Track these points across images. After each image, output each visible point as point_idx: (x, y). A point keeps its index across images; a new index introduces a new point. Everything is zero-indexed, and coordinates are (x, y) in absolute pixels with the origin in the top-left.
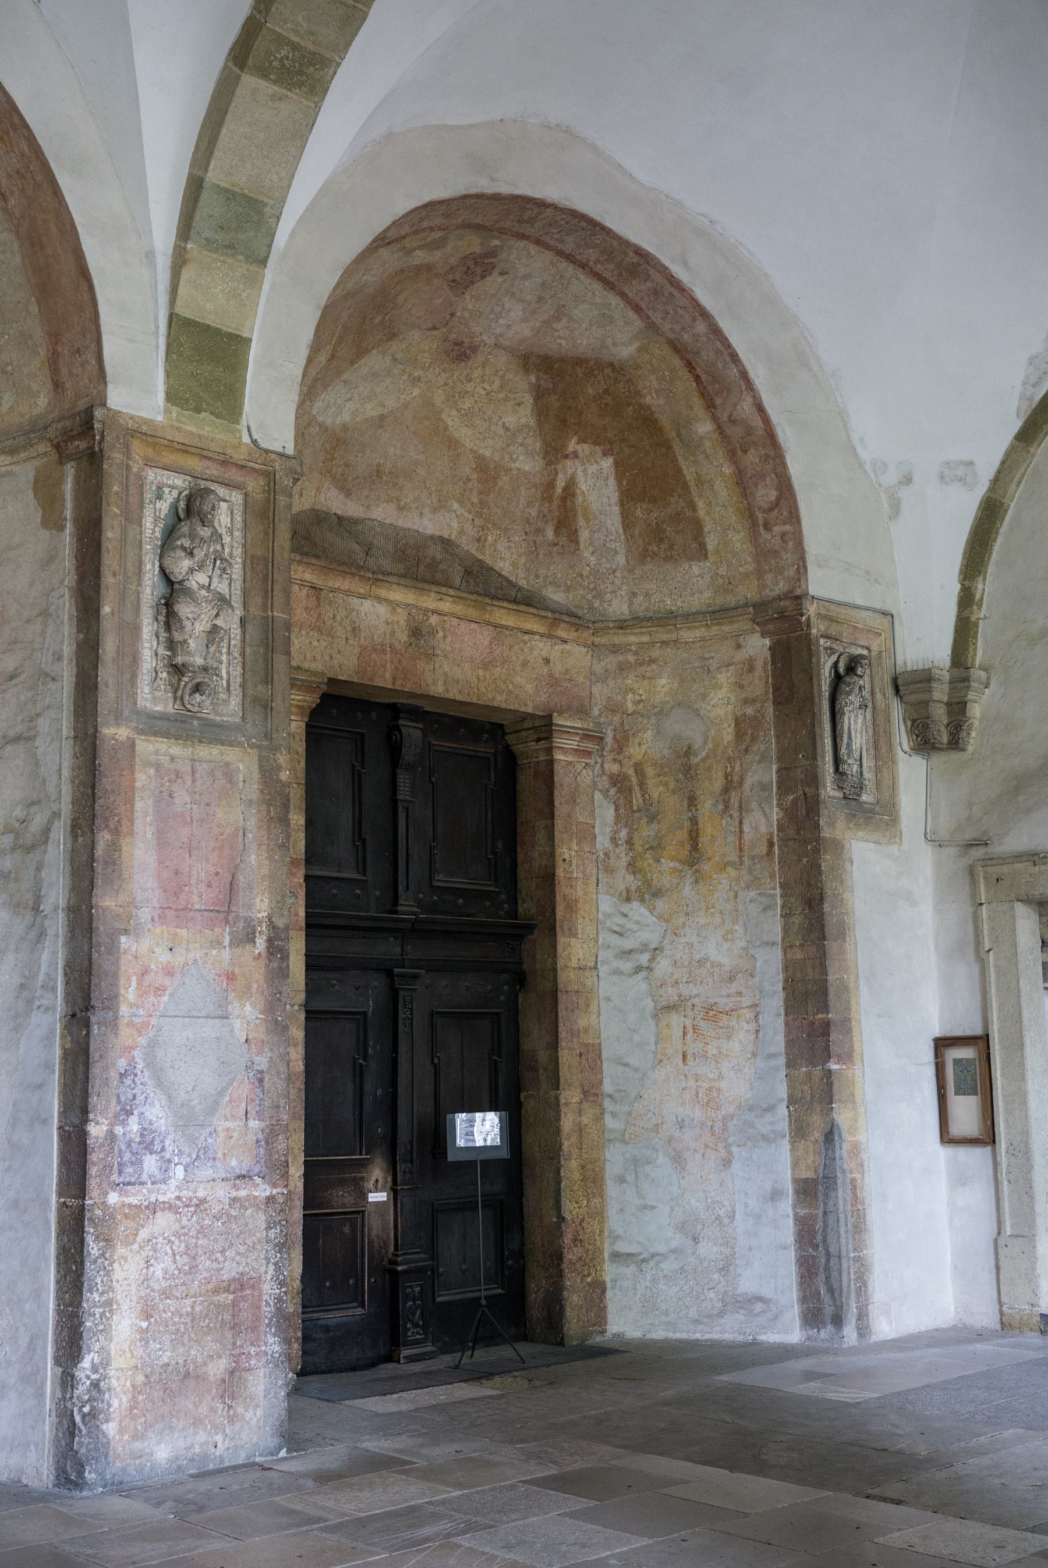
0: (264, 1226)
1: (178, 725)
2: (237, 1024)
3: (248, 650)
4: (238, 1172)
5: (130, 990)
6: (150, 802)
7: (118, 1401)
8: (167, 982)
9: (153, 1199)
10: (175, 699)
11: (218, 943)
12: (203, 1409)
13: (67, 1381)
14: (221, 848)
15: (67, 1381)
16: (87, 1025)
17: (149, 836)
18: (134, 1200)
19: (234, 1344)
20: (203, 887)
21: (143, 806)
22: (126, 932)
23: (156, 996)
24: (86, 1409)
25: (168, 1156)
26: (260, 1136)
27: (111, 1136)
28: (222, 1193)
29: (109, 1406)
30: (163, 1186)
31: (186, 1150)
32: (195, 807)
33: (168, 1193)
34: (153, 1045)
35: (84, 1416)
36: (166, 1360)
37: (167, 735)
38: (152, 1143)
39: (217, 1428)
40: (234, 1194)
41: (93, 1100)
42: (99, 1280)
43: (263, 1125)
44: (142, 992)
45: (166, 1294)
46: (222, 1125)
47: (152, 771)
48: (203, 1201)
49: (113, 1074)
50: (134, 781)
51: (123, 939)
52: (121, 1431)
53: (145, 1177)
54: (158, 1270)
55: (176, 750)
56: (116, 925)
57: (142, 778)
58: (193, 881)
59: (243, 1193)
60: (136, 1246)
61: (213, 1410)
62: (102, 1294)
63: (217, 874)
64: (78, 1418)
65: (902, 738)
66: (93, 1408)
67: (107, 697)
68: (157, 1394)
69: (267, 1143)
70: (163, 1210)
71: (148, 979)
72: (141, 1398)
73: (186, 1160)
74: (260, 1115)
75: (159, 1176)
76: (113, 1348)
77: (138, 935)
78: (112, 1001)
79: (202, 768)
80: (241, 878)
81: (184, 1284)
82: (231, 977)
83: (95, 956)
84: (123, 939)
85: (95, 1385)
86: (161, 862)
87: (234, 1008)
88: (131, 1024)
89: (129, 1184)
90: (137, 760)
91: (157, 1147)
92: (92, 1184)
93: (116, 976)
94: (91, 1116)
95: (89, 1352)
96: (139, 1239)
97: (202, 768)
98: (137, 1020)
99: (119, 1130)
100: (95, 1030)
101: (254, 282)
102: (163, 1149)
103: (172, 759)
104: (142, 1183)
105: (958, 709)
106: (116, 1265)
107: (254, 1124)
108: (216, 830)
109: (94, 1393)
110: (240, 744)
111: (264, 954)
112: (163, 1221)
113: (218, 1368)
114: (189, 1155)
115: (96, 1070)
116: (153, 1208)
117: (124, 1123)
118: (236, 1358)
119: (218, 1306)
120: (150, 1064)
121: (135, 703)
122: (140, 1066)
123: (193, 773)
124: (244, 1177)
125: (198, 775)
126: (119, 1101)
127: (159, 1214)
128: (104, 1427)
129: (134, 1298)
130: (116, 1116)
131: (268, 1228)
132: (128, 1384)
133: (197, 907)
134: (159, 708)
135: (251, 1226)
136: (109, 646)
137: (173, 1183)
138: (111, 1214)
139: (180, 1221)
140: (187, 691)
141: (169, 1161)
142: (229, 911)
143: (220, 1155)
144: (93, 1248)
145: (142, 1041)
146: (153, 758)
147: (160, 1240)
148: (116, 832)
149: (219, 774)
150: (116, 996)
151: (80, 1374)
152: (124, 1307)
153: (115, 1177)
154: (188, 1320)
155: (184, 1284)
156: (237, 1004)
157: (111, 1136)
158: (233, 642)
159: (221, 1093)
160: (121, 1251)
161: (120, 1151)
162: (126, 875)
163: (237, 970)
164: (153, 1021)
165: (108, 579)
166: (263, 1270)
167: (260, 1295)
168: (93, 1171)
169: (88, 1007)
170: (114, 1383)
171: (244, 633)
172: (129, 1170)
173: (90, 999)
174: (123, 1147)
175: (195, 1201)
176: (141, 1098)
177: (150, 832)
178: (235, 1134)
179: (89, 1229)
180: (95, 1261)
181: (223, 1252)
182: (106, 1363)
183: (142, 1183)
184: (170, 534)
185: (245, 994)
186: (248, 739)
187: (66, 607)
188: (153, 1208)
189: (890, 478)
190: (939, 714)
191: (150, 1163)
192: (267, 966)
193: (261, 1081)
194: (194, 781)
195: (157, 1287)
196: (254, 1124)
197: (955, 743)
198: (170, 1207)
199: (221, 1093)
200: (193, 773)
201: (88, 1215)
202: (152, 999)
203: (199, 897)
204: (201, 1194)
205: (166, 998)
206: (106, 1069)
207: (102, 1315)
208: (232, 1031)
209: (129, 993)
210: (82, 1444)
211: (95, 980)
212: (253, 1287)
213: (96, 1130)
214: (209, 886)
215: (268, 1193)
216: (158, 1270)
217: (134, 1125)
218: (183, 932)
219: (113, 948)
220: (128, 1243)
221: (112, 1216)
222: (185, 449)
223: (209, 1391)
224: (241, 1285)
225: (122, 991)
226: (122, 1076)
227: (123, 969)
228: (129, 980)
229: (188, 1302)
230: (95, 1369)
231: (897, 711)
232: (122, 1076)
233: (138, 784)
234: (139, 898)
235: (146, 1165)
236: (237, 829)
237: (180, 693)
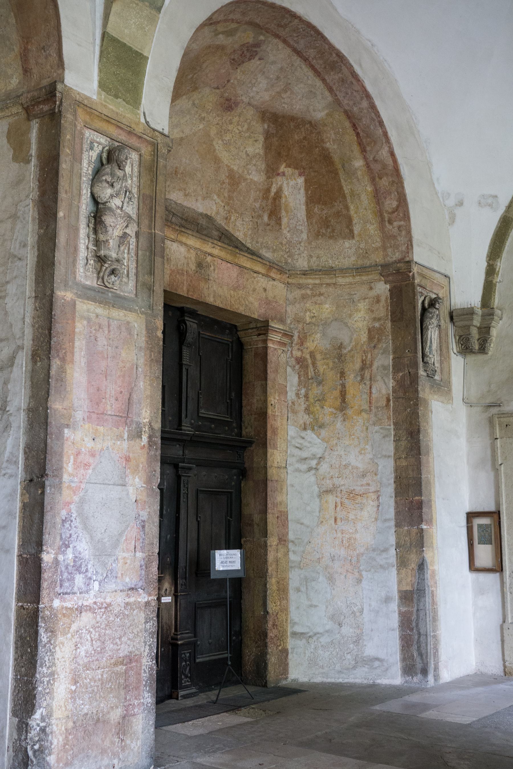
0: (143, 621)
1: (100, 294)
2: (131, 490)
3: (140, 252)
4: (129, 586)
5: (70, 465)
6: (84, 342)
8: (91, 460)
9: (80, 604)
10: (98, 278)
11: (120, 437)
12: (107, 743)
14: (124, 376)
16: (43, 486)
17: (83, 364)
18: (69, 605)
19: (126, 699)
20: (113, 400)
22: (68, 426)
23: (84, 469)
24: (36, 747)
25: (89, 575)
26: (143, 563)
27: (56, 562)
29: (51, 744)
30: (86, 595)
31: (100, 571)
32: (109, 348)
34: (82, 501)
35: (35, 752)
36: (86, 711)
37: (94, 300)
38: (80, 566)
39: (115, 755)
40: (127, 600)
41: (46, 537)
42: (46, 659)
43: (144, 555)
44: (77, 467)
45: (87, 667)
46: (121, 555)
47: (85, 322)
48: (109, 605)
49: (58, 520)
50: (74, 328)
51: (66, 431)
52: (58, 761)
53: (76, 589)
54: (82, 651)
55: (100, 310)
56: (62, 421)
57: (80, 326)
58: (108, 396)
59: (132, 600)
60: (69, 635)
61: (113, 743)
62: (48, 668)
63: (121, 392)
64: (30, 753)
66: (41, 746)
68: (80, 734)
69: (146, 568)
70: (86, 611)
71: (80, 458)
72: (70, 737)
73: (100, 578)
74: (142, 550)
75: (84, 589)
76: (55, 704)
77: (75, 429)
78: (59, 471)
79: (114, 324)
80: (134, 396)
81: (97, 660)
82: (128, 459)
83: (49, 441)
84: (66, 431)
85: (43, 730)
86: (89, 382)
87: (129, 479)
88: (69, 487)
89: (66, 593)
90: (77, 314)
91: (83, 569)
92: (44, 593)
93: (61, 455)
94: (44, 548)
95: (40, 707)
96: (71, 630)
97: (114, 324)
98: (73, 485)
99: (61, 558)
100: (48, 490)
102: (87, 571)
103: (97, 316)
104: (74, 593)
106: (57, 648)
107: (139, 555)
108: (121, 365)
109: (42, 736)
110: (135, 311)
111: (147, 446)
113: (116, 715)
114: (102, 575)
115: (48, 517)
116: (80, 610)
117: (64, 553)
118: (127, 708)
119: (117, 674)
120: (80, 514)
121: (75, 278)
122: (74, 515)
123: (109, 326)
124: (133, 589)
125: (111, 328)
126: (61, 538)
127: (83, 614)
128: (48, 759)
129: (68, 670)
130: (59, 548)
131: (146, 622)
132: (63, 729)
133: (109, 413)
134: (88, 283)
135: (136, 621)
137: (92, 593)
138: (54, 614)
139: (95, 618)
140: (107, 273)
141: (90, 578)
142: (127, 417)
143: (119, 575)
144: (43, 637)
145: (76, 498)
146: (86, 314)
147: (84, 631)
148: (63, 360)
149: (123, 329)
150: (61, 468)
151: (32, 723)
152: (62, 676)
153: (58, 589)
154: (99, 684)
155: (97, 660)
156: (130, 477)
157: (56, 562)
158: (131, 247)
159: (121, 535)
160: (60, 638)
161: (61, 572)
162: (68, 389)
163: (131, 455)
164: (83, 486)
166: (143, 649)
167: (141, 666)
168: (45, 585)
169: (43, 474)
170: (55, 728)
171: (138, 242)
172: (66, 584)
173: (45, 470)
174: (63, 569)
175: (105, 605)
176: (74, 536)
177: (83, 361)
178: (128, 561)
179: (41, 624)
180: (45, 646)
181: (120, 638)
182: (50, 715)
183: (74, 593)
185: (135, 471)
186: (140, 308)
188: (80, 610)
191: (79, 580)
192: (148, 453)
193: (143, 527)
194: (109, 331)
195: (81, 663)
196: (139, 555)
198: (90, 609)
199: (121, 535)
200: (109, 326)
201: (41, 615)
202: (82, 471)
204: (108, 600)
205: (90, 471)
206: (54, 516)
207: (48, 682)
208: (128, 494)
211: (48, 457)
212: (136, 661)
213: (47, 557)
214: (117, 400)
215: (146, 600)
216: (82, 651)
217: (70, 555)
218: (101, 429)
219: (60, 436)
220: (64, 633)
221: (56, 615)
223: (111, 730)
225: (65, 465)
226: (64, 521)
227: (65, 451)
228: (69, 458)
229: (99, 672)
230: (43, 719)
232: (64, 521)
233: (77, 330)
234: (76, 405)
235: (76, 581)
236: (133, 365)
237: (101, 274)
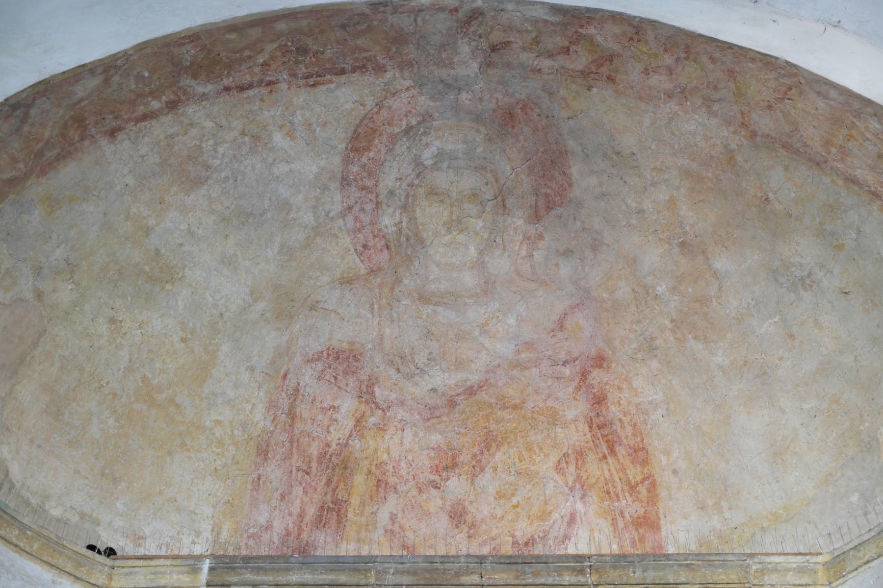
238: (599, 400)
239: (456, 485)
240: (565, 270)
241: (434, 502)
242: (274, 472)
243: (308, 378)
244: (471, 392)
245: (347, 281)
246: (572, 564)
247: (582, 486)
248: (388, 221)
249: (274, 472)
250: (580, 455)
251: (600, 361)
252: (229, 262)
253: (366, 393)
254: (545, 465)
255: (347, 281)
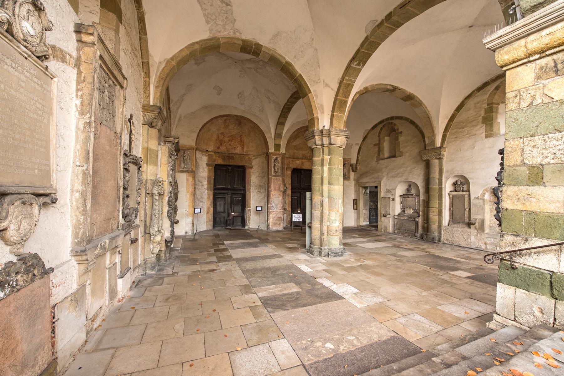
7: (271, 225)
13: (267, 223)
15: (267, 223)
21: (272, 182)
28: (279, 211)
33: (275, 210)
65: (351, 170)
67: (269, 174)
101: (281, 140)
105: (356, 168)
112: (274, 212)
136: (269, 170)
165: (269, 165)
184: (275, 161)
187: (267, 167)
189: (350, 145)
190: (354, 168)
191: (273, 208)
197: (356, 171)
203: (277, 189)
209: (271, 196)
210: (268, 227)
222: (276, 154)
224: (280, 217)
231: (351, 168)
238: (241, 138)
239: (230, 142)
240: (240, 129)
241: (228, 143)
242: (217, 142)
243: (220, 135)
244: (232, 136)
245: (223, 128)
246: (236, 169)
247: (239, 144)
248: (227, 124)
249: (217, 142)
250: (239, 142)
251: (242, 135)
252: (214, 128)
253: (224, 135)
254: (236, 142)
255: (223, 128)
